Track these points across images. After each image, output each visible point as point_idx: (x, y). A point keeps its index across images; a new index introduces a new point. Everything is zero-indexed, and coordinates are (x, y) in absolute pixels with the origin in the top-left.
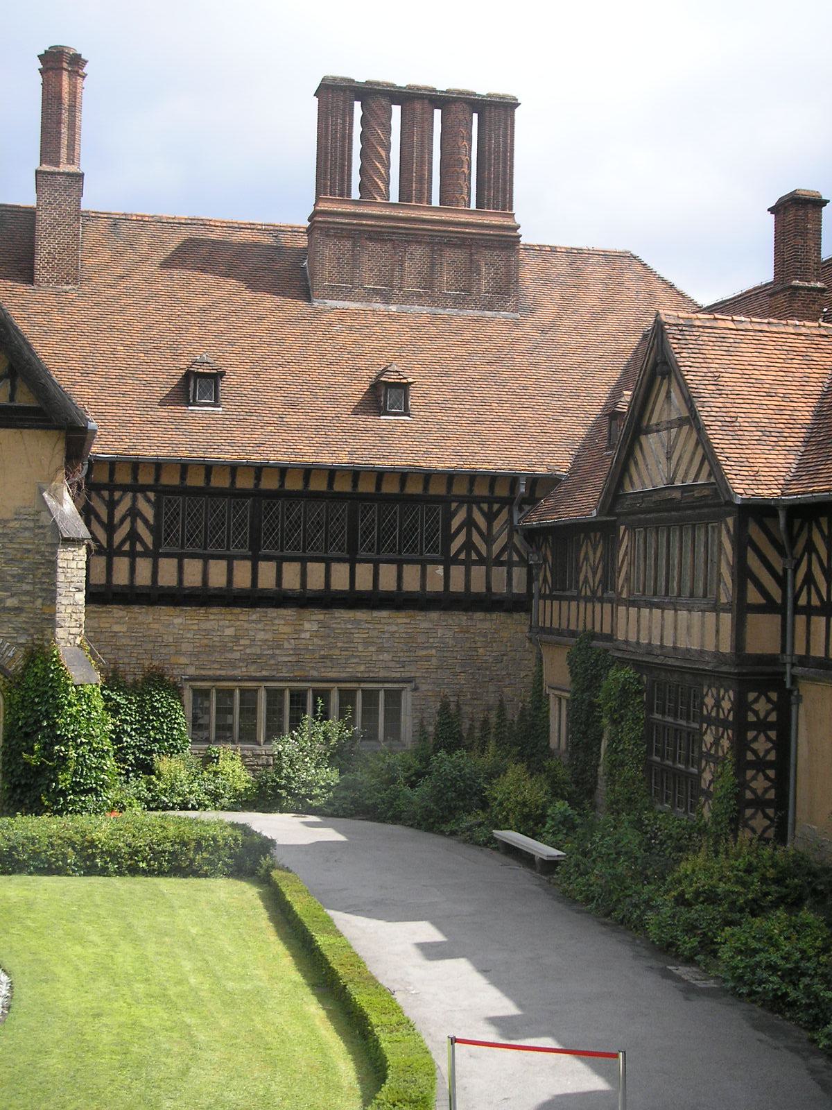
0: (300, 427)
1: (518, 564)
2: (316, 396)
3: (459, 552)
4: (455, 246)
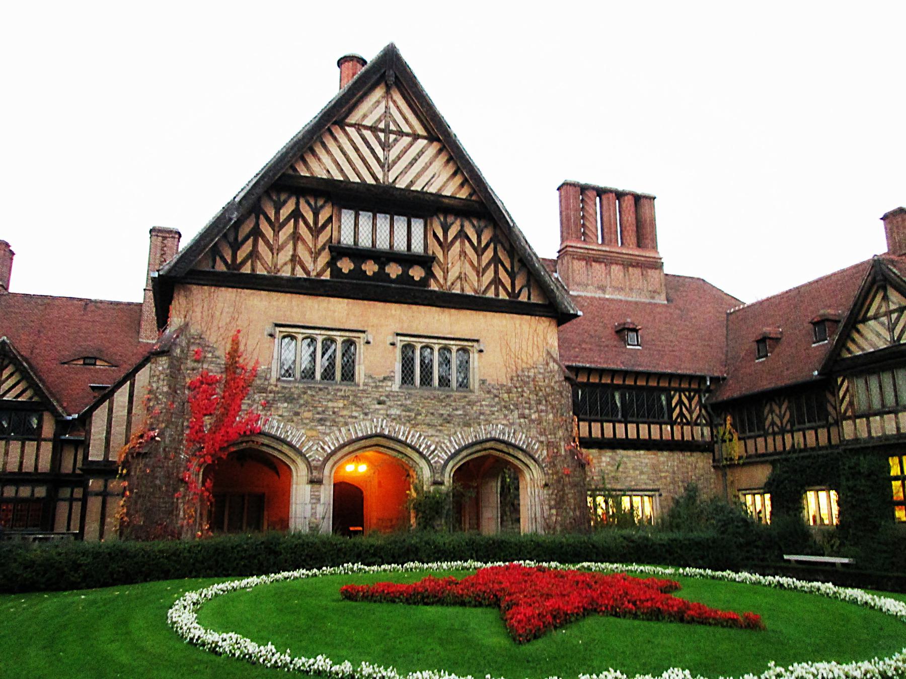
0: (590, 349)
1: (705, 425)
2: (592, 337)
3: (677, 418)
4: (633, 266)
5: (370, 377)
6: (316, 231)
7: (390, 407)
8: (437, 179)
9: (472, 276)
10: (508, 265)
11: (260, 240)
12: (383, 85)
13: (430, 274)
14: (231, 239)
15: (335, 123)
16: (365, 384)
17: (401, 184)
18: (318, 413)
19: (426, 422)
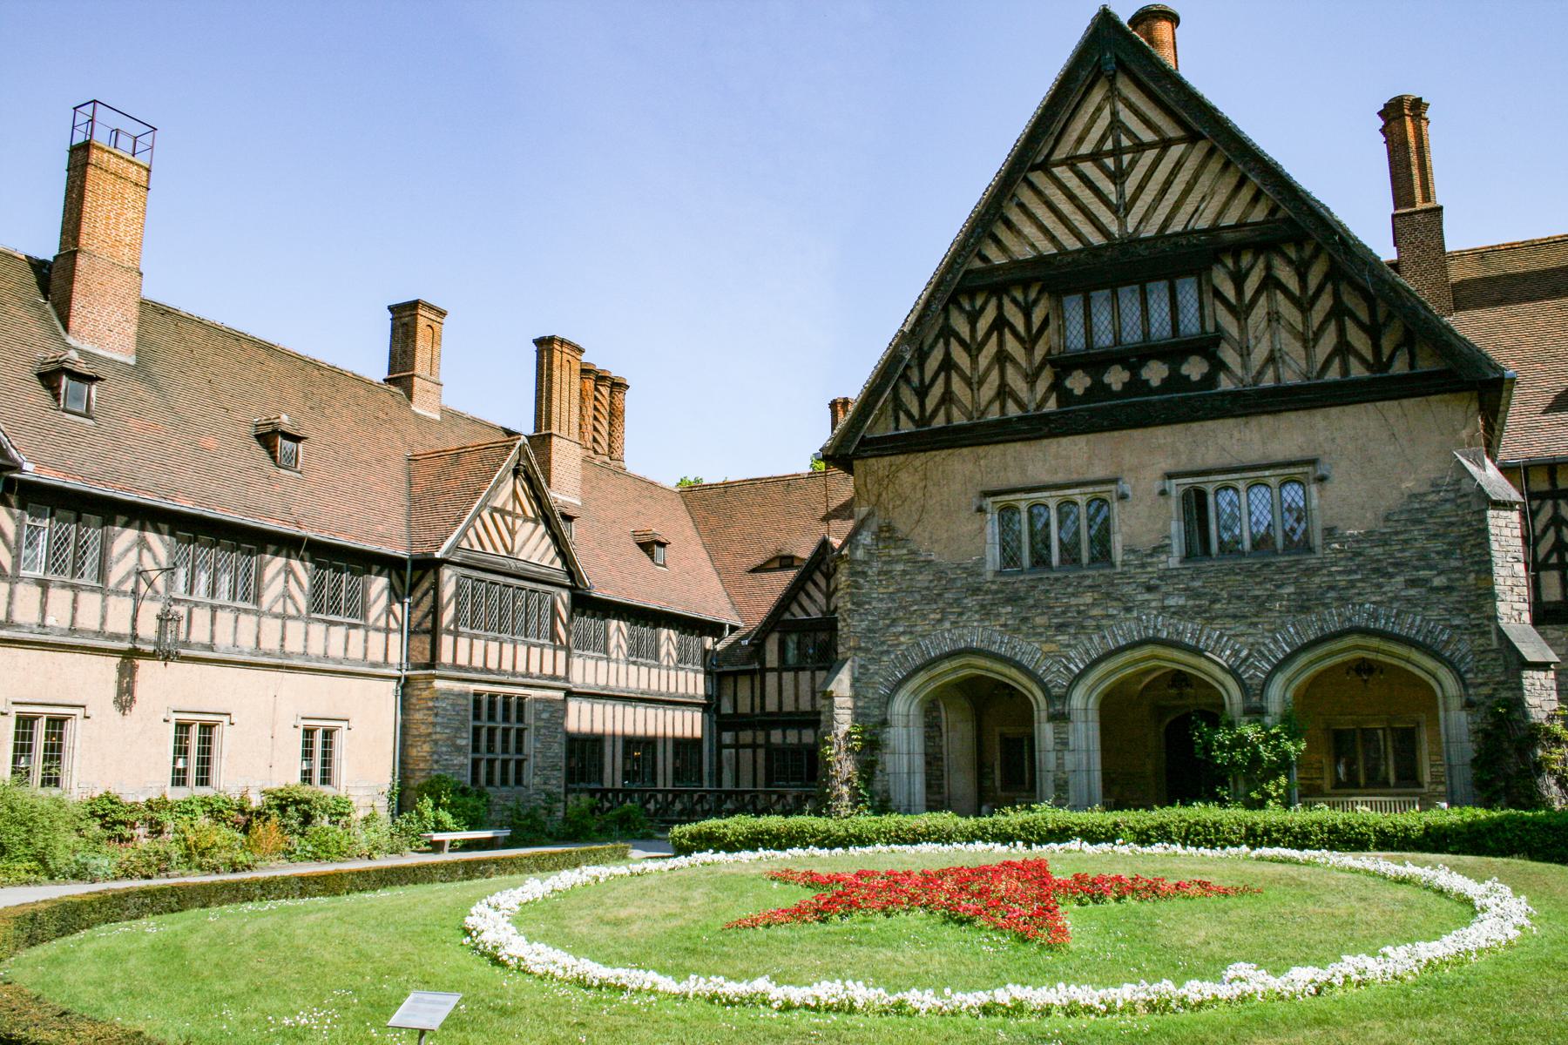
5: (1134, 551)
6: (1029, 342)
7: (1167, 595)
8: (1209, 204)
9: (1294, 349)
10: (1364, 316)
11: (954, 375)
12: (1103, 79)
13: (1218, 366)
14: (916, 380)
15: (1034, 168)
16: (1124, 563)
17: (1150, 231)
18: (1056, 616)
19: (1231, 611)
